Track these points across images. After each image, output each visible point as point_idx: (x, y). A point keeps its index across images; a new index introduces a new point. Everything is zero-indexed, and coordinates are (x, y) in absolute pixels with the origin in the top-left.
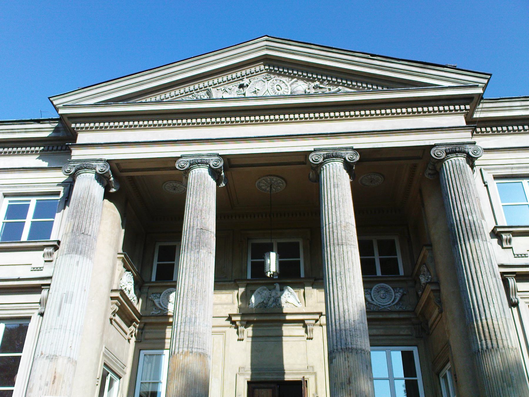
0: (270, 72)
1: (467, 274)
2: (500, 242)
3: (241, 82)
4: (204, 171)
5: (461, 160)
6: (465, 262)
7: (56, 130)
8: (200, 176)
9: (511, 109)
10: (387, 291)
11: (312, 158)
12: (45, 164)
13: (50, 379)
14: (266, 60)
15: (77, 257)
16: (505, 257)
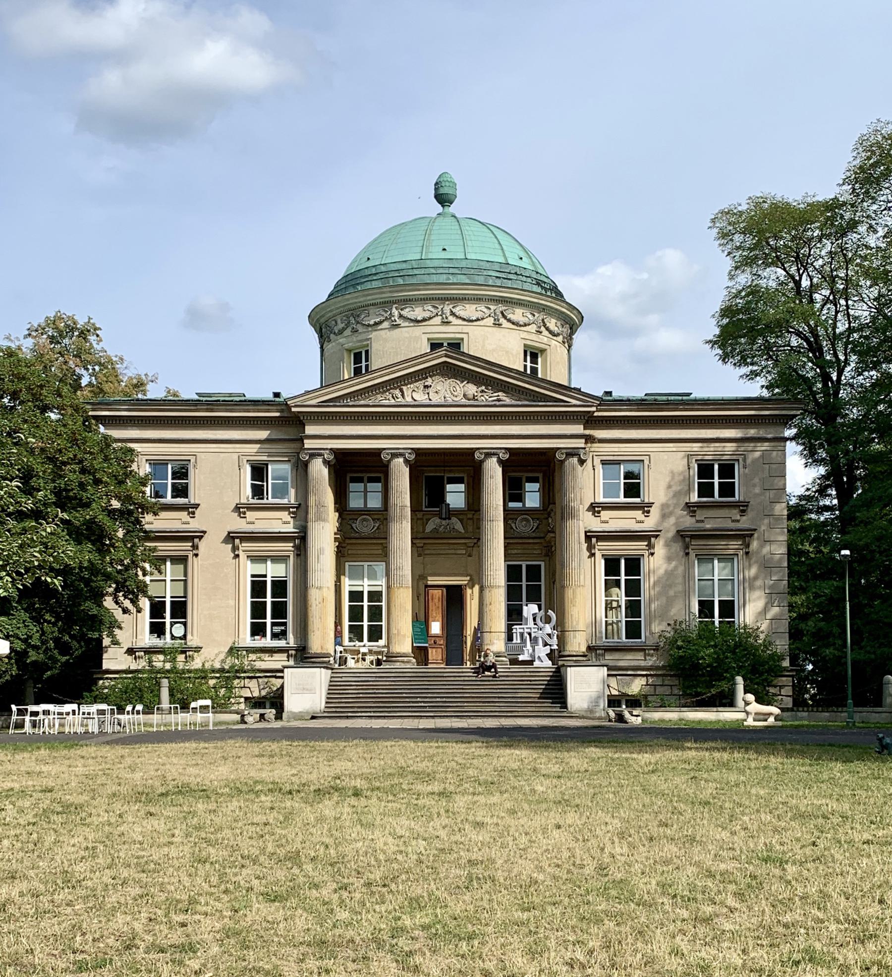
3: (426, 384)
4: (401, 460)
5: (575, 460)
10: (527, 520)
11: (477, 455)
13: (321, 600)
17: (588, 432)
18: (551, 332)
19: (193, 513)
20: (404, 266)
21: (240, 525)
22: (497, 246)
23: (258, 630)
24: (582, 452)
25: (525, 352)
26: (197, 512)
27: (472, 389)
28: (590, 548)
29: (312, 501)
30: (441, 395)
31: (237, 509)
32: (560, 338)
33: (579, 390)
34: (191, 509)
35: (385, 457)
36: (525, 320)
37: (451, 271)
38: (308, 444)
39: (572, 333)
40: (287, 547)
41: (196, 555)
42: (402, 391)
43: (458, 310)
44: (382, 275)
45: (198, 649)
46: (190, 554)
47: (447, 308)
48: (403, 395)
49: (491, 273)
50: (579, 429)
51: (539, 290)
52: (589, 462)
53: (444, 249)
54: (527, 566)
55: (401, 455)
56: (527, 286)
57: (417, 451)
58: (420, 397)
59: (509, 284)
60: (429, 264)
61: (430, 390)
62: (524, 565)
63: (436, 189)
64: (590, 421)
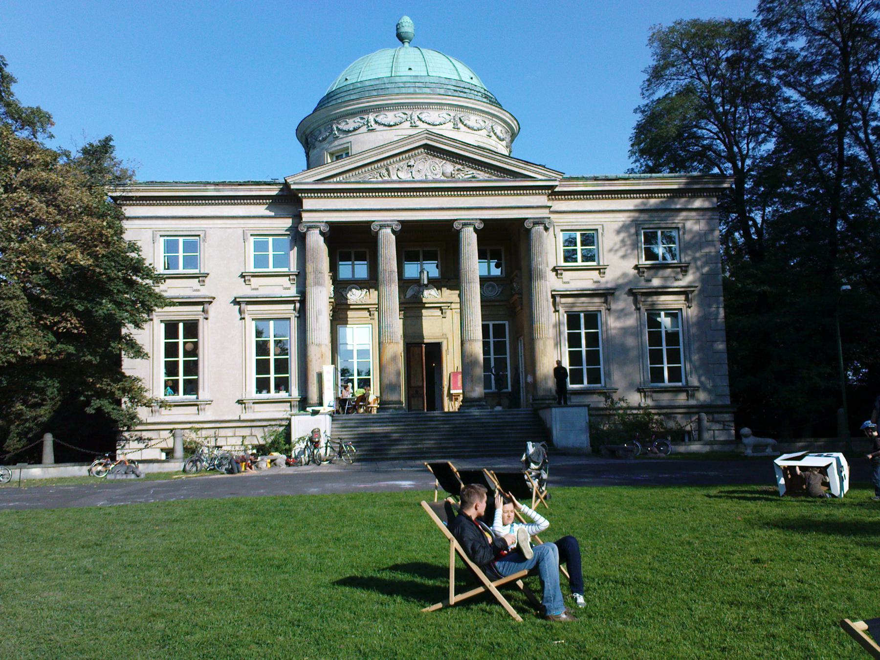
0: (428, 154)
1: (535, 299)
2: (557, 275)
5: (541, 227)
6: (534, 292)
7: (281, 190)
8: (387, 234)
9: (577, 186)
10: (493, 287)
11: (456, 225)
12: (273, 214)
14: (425, 146)
15: (320, 288)
17: (549, 204)
18: (498, 137)
19: (204, 281)
20: (377, 82)
21: (244, 291)
22: (452, 67)
23: (262, 385)
24: (547, 222)
26: (207, 280)
27: (449, 168)
28: (554, 304)
29: (310, 268)
30: (423, 173)
31: (242, 276)
33: (544, 167)
34: (201, 277)
35: (374, 227)
36: (479, 126)
37: (417, 85)
38: (306, 217)
39: (512, 141)
40: (288, 310)
41: (207, 319)
42: (387, 170)
43: (422, 117)
44: (358, 90)
45: (209, 402)
46: (201, 318)
47: (416, 114)
48: (389, 175)
49: (449, 87)
50: (542, 200)
52: (551, 230)
53: (410, 69)
54: (494, 325)
55: (388, 226)
56: (477, 98)
57: (402, 222)
58: (404, 175)
59: (465, 95)
60: (398, 79)
61: (413, 169)
62: (491, 324)
63: (397, 29)
64: (553, 193)
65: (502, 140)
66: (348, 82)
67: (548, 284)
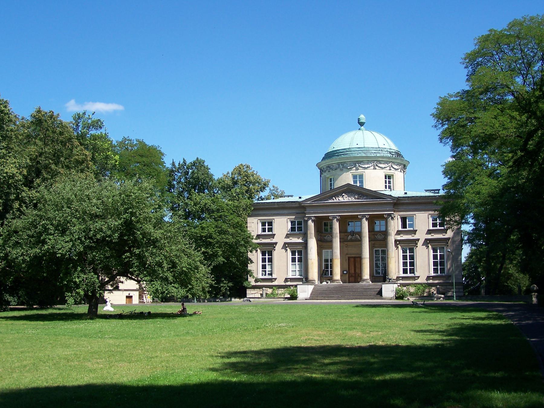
16: (399, 238)
18: (395, 169)
20: (344, 151)
25: (386, 176)
32: (399, 170)
51: (389, 155)
65: (398, 169)
66: (334, 149)
67: (392, 239)
